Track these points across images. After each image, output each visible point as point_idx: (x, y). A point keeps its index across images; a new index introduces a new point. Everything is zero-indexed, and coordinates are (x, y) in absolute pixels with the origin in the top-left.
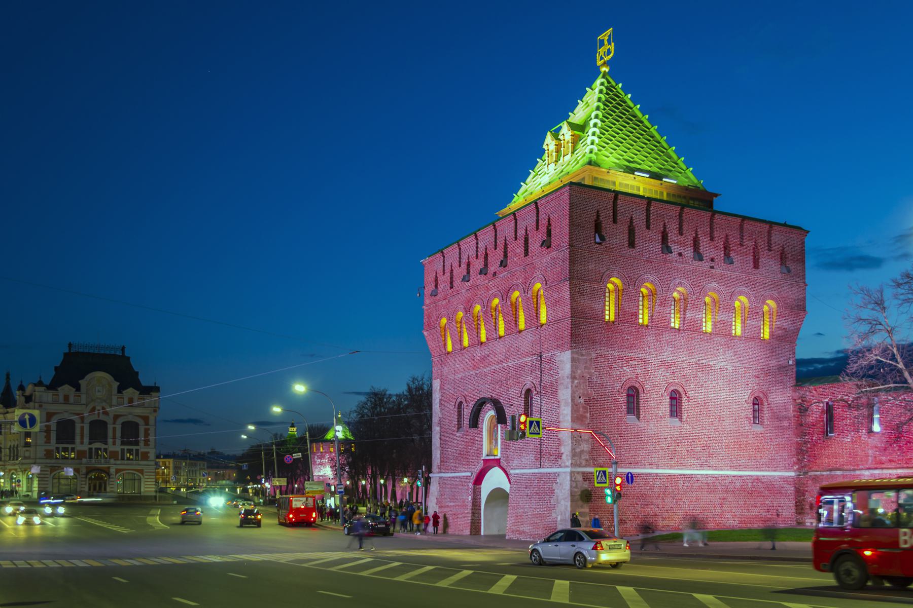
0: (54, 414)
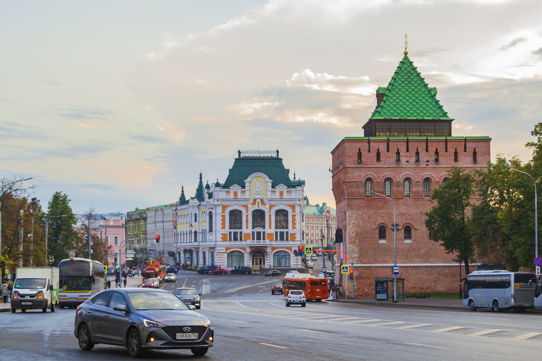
0: (227, 206)
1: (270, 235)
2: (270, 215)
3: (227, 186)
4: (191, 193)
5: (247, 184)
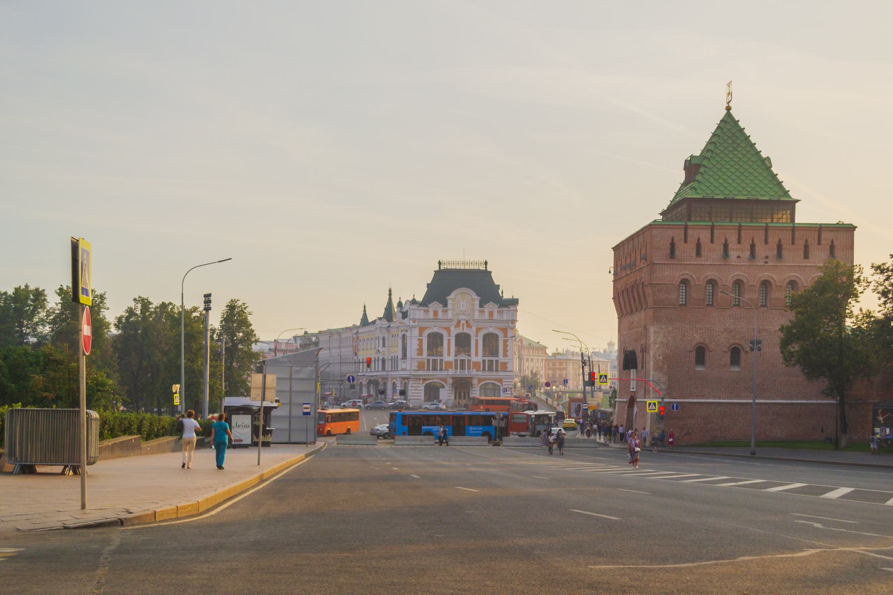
1: (476, 365)
2: (477, 341)
3: (425, 303)
4: (376, 313)
5: (450, 302)
